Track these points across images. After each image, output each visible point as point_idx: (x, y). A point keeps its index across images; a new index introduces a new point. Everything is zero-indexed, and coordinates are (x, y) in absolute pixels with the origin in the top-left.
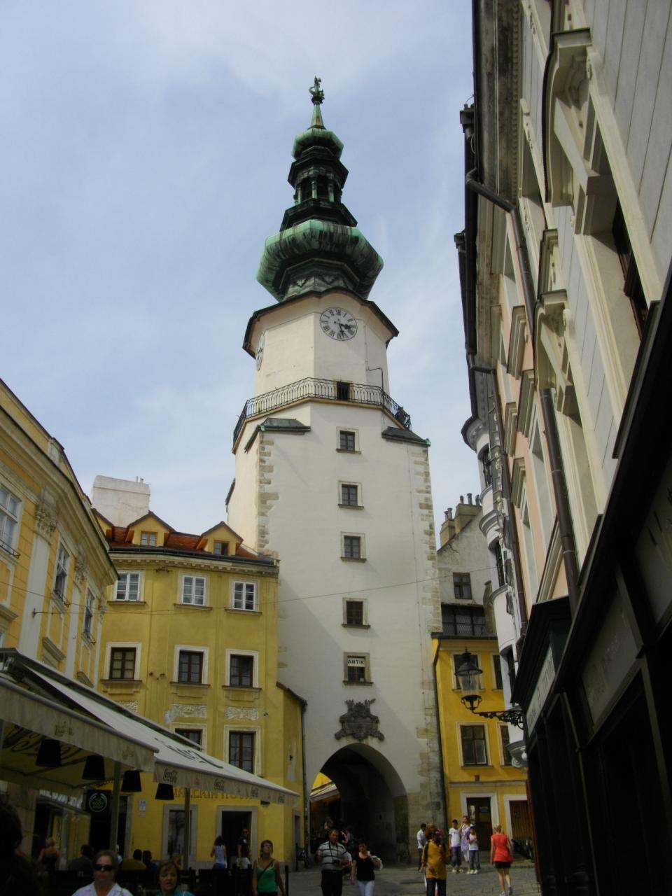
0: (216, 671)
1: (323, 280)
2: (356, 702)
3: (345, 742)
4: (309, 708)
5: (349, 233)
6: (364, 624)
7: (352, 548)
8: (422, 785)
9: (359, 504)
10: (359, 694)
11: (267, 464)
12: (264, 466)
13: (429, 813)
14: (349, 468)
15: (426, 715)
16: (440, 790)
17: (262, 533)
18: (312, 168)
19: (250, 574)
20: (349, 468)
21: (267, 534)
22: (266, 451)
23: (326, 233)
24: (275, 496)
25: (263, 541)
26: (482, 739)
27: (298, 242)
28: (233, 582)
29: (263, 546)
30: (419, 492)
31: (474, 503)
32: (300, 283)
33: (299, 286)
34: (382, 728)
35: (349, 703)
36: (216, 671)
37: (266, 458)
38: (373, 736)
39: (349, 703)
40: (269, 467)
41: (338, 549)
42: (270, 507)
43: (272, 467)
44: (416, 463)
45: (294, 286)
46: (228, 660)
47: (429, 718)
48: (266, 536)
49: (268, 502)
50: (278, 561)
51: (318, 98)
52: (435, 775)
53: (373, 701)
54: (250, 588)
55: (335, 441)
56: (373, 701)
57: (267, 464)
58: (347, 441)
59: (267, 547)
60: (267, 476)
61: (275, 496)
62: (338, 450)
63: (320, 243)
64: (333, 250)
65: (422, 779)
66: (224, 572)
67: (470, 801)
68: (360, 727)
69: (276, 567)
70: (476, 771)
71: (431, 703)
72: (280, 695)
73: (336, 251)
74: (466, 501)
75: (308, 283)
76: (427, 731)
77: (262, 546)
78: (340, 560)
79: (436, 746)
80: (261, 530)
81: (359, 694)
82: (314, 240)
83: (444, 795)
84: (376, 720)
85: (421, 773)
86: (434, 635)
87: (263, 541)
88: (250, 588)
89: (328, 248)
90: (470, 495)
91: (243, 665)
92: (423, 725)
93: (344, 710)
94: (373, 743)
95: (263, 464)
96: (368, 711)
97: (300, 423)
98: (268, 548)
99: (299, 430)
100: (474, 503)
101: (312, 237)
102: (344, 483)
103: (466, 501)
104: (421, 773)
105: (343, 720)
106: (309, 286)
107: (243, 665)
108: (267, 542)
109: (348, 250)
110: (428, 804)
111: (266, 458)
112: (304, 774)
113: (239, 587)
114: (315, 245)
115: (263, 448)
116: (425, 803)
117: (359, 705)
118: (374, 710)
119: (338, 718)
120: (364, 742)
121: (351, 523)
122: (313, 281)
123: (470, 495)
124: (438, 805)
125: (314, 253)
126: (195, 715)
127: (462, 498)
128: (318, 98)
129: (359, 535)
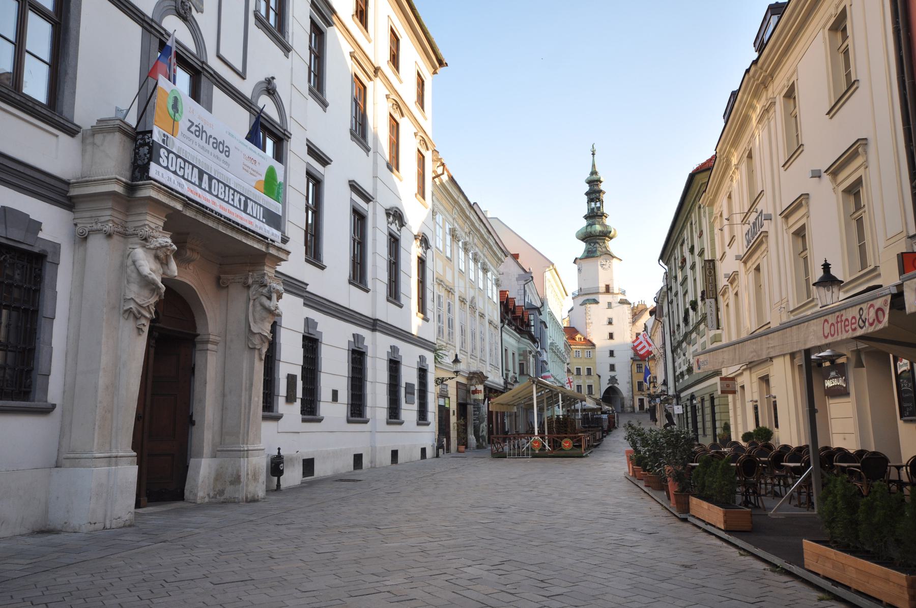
0: (584, 372)
3: (609, 385)
4: (601, 377)
7: (611, 336)
10: (613, 374)
13: (629, 402)
14: (610, 313)
20: (610, 313)
28: (586, 351)
31: (643, 303)
32: (592, 244)
34: (618, 382)
35: (611, 376)
36: (584, 372)
39: (611, 376)
51: (593, 154)
52: (631, 393)
54: (590, 352)
55: (606, 306)
58: (610, 305)
65: (628, 394)
67: (639, 399)
70: (640, 392)
71: (630, 375)
72: (597, 376)
79: (631, 386)
81: (613, 374)
83: (633, 398)
84: (617, 380)
88: (590, 352)
91: (589, 370)
93: (609, 378)
94: (616, 385)
100: (643, 303)
105: (609, 380)
107: (589, 370)
114: (598, 234)
118: (616, 377)
119: (608, 379)
121: (610, 329)
128: (593, 154)
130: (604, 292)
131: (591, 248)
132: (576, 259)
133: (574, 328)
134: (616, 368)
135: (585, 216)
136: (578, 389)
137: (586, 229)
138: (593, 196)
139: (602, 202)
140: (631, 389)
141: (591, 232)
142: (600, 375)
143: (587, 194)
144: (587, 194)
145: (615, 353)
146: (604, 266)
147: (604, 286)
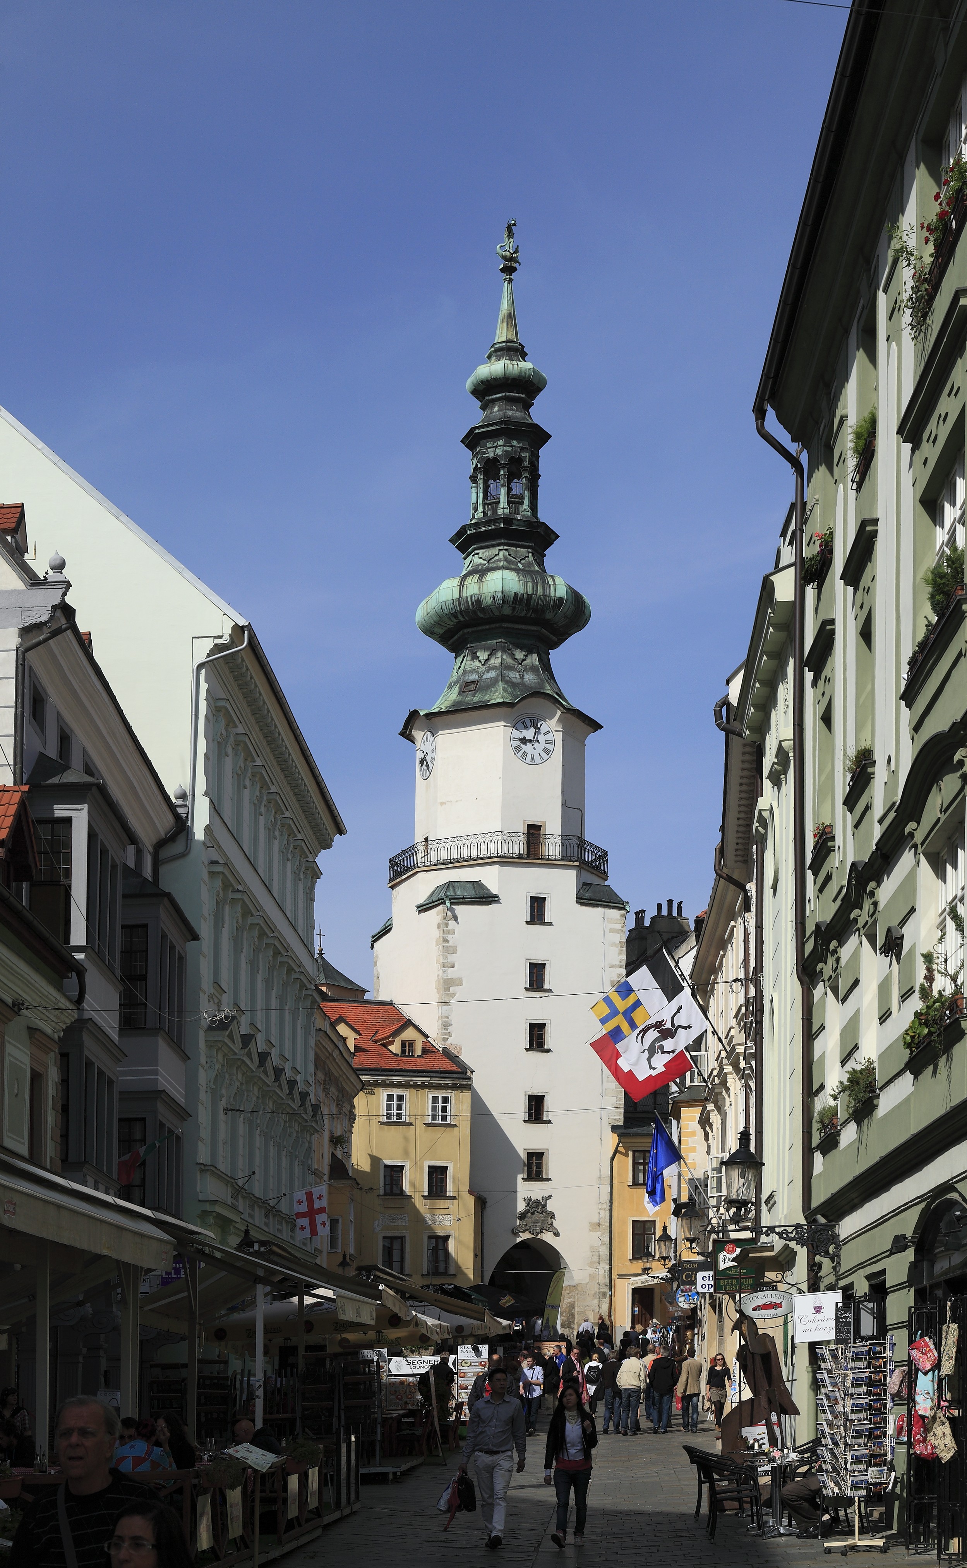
1: (512, 656)
2: (533, 1198)
4: (488, 1205)
5: (552, 594)
6: (545, 1119)
8: (590, 1275)
9: (546, 986)
11: (451, 943)
12: (447, 947)
15: (600, 1209)
16: (608, 1281)
17: (446, 1025)
18: (501, 442)
19: (446, 1087)
21: (451, 1025)
22: (450, 927)
23: (522, 596)
24: (458, 982)
25: (445, 1034)
26: (653, 1234)
27: (484, 605)
29: (448, 1039)
30: (612, 967)
32: (483, 655)
33: (480, 661)
34: (556, 1224)
37: (449, 937)
38: (548, 1231)
40: (453, 947)
41: (523, 1039)
42: (454, 995)
43: (456, 947)
44: (612, 931)
45: (472, 659)
46: (426, 1170)
47: (602, 1212)
48: (449, 1028)
49: (452, 988)
50: (472, 1072)
52: (605, 1267)
53: (550, 1197)
56: (550, 1197)
57: (451, 943)
59: (450, 1040)
60: (452, 958)
61: (458, 982)
62: (527, 923)
63: (514, 609)
64: (529, 615)
65: (591, 1271)
66: (423, 1086)
68: (536, 1222)
69: (470, 1079)
73: (533, 616)
74: (665, 912)
75: (492, 661)
76: (599, 1224)
77: (445, 1039)
78: (525, 1050)
79: (607, 1239)
80: (445, 1022)
82: (506, 606)
85: (591, 1265)
86: (614, 1128)
87: (445, 1034)
89: (523, 614)
90: (670, 902)
92: (596, 1220)
94: (547, 1237)
95: (446, 944)
96: (545, 1206)
97: (488, 890)
98: (452, 1042)
99: (485, 898)
101: (504, 602)
102: (532, 962)
103: (665, 912)
104: (591, 1265)
106: (494, 668)
108: (450, 1035)
109: (549, 615)
110: (595, 1293)
111: (449, 937)
112: (482, 1268)
113: (435, 1100)
115: (447, 925)
116: (593, 1292)
117: (537, 1202)
118: (550, 1207)
120: (539, 1237)
122: (500, 660)
123: (670, 902)
124: (604, 1294)
125: (503, 619)
126: (399, 1223)
127: (660, 906)
129: (544, 1022)
130: (520, 856)
131: (473, 671)
132: (414, 714)
133: (390, 1004)
134: (552, 1166)
135: (459, 534)
136: (388, 1252)
137: (461, 585)
138: (497, 449)
139: (535, 477)
140: (605, 1252)
141: (478, 601)
142: (484, 1195)
143: (473, 440)
144: (473, 440)
145: (550, 1109)
146: (528, 748)
147: (522, 829)
